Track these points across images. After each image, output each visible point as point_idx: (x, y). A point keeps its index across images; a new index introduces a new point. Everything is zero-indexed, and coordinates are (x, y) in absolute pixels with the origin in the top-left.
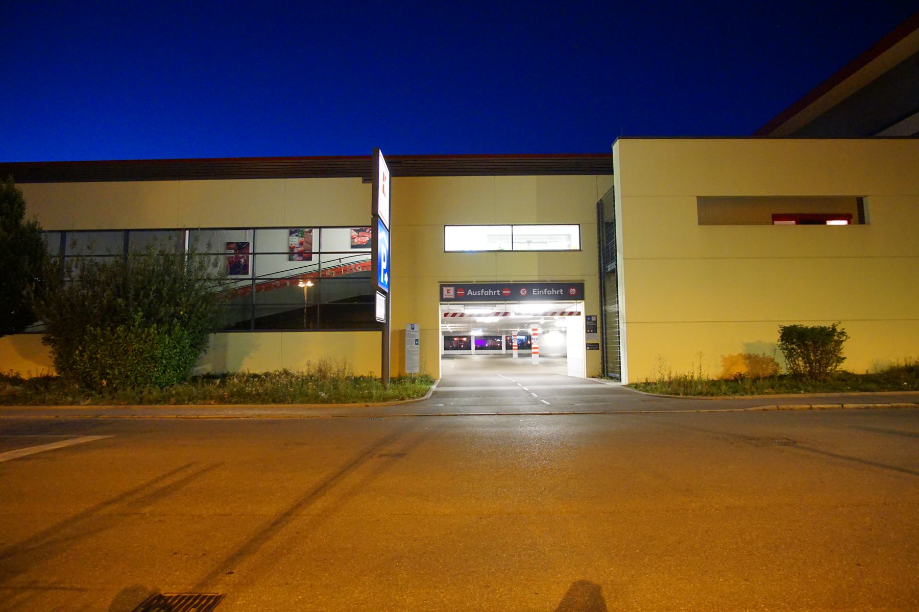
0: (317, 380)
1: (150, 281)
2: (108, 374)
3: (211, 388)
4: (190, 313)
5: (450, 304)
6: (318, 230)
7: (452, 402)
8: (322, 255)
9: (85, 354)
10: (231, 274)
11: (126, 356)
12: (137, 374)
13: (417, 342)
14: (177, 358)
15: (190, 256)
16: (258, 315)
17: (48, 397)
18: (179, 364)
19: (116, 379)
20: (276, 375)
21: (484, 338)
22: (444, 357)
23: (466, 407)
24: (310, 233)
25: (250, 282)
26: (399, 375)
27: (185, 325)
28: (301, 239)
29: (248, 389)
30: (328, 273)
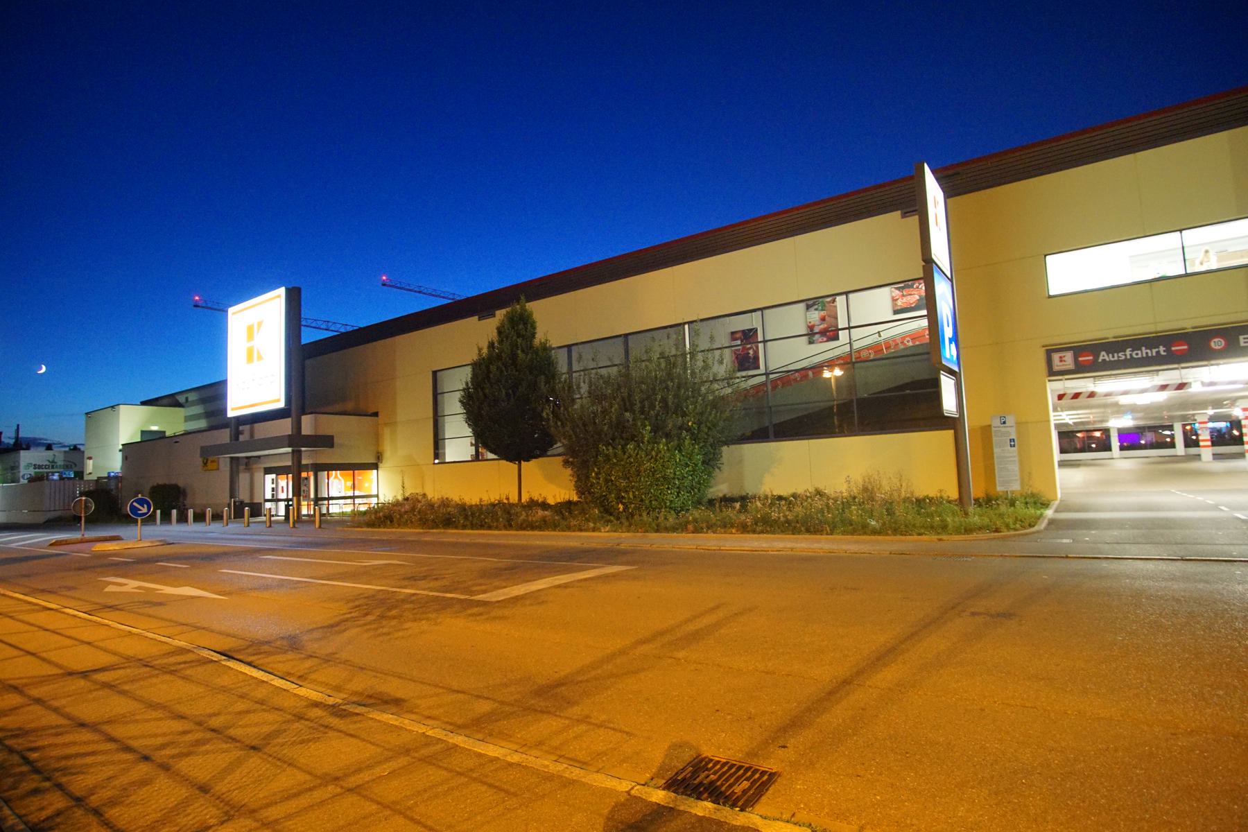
0: (863, 502)
1: (654, 389)
2: (623, 497)
3: (731, 513)
4: (699, 423)
5: (1066, 379)
6: (845, 296)
7: (1088, 536)
8: (852, 330)
9: (600, 476)
10: (739, 370)
11: (639, 477)
12: (651, 497)
13: (1012, 443)
14: (690, 477)
15: (693, 354)
16: (776, 420)
17: (573, 522)
18: (692, 485)
19: (631, 503)
20: (806, 496)
21: (1138, 431)
22: (1063, 464)
23: (1115, 545)
24: (833, 303)
25: (763, 378)
26: (987, 495)
27: (695, 438)
28: (823, 313)
29: (774, 515)
30: (864, 354)
